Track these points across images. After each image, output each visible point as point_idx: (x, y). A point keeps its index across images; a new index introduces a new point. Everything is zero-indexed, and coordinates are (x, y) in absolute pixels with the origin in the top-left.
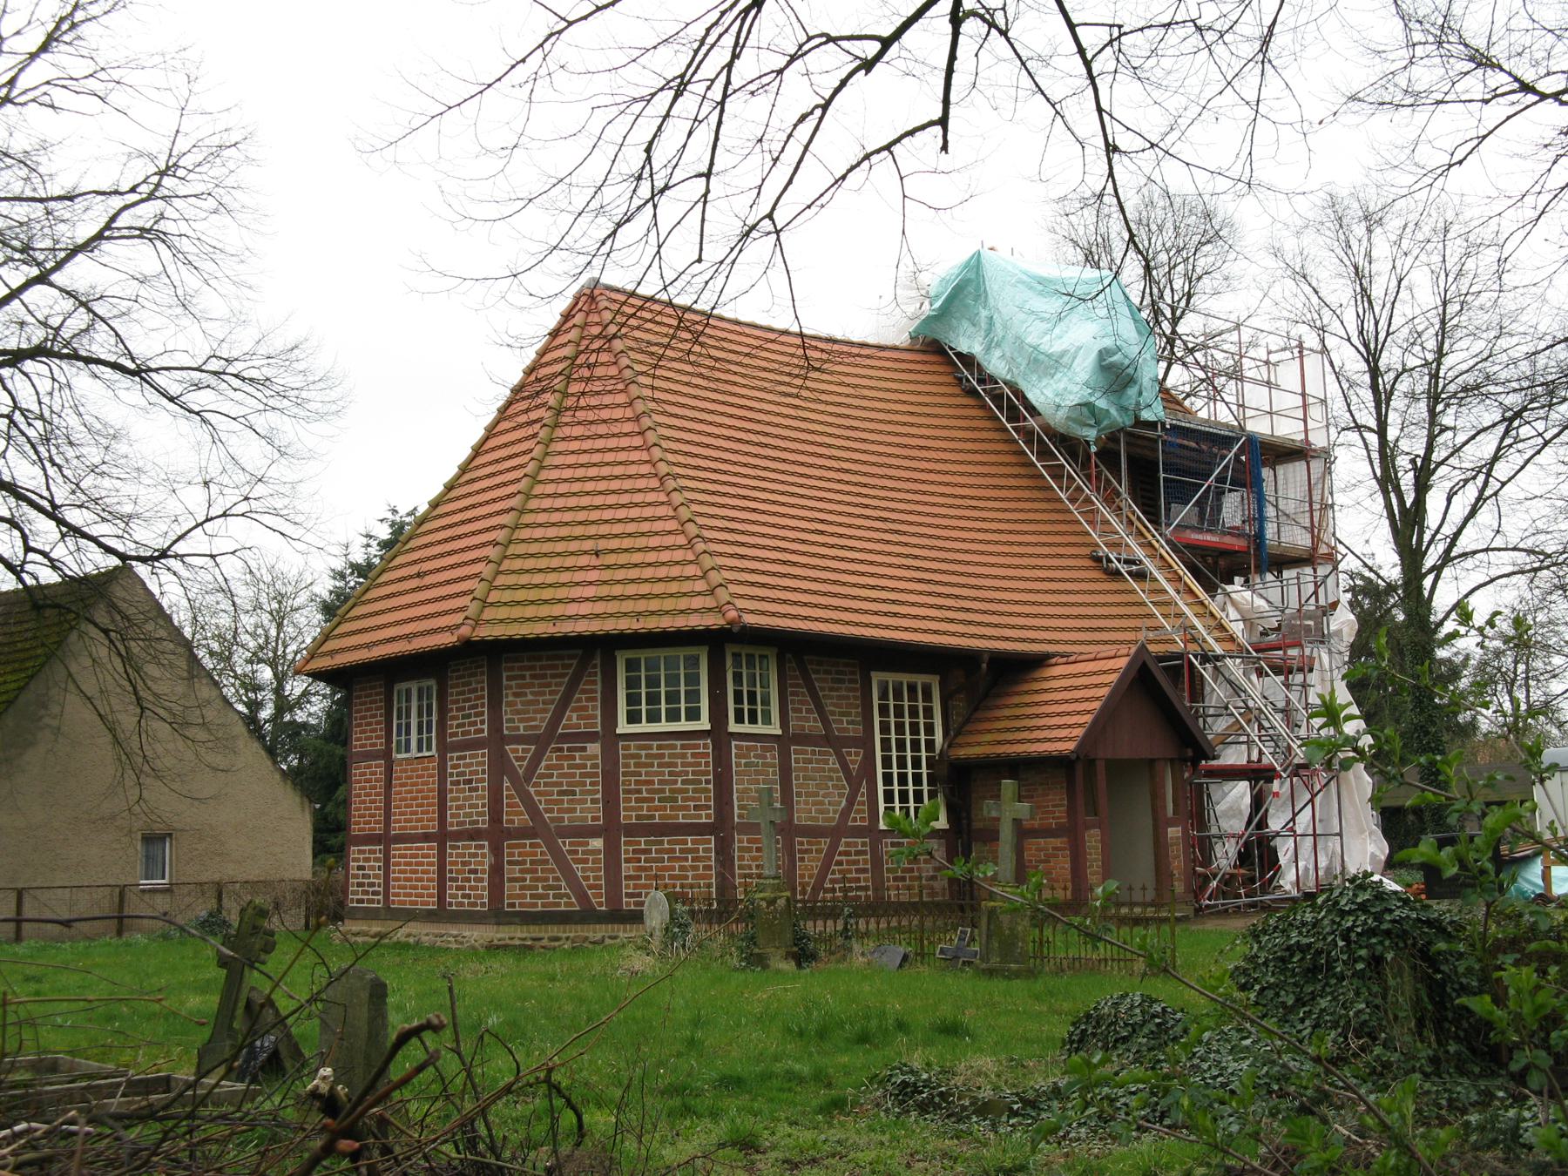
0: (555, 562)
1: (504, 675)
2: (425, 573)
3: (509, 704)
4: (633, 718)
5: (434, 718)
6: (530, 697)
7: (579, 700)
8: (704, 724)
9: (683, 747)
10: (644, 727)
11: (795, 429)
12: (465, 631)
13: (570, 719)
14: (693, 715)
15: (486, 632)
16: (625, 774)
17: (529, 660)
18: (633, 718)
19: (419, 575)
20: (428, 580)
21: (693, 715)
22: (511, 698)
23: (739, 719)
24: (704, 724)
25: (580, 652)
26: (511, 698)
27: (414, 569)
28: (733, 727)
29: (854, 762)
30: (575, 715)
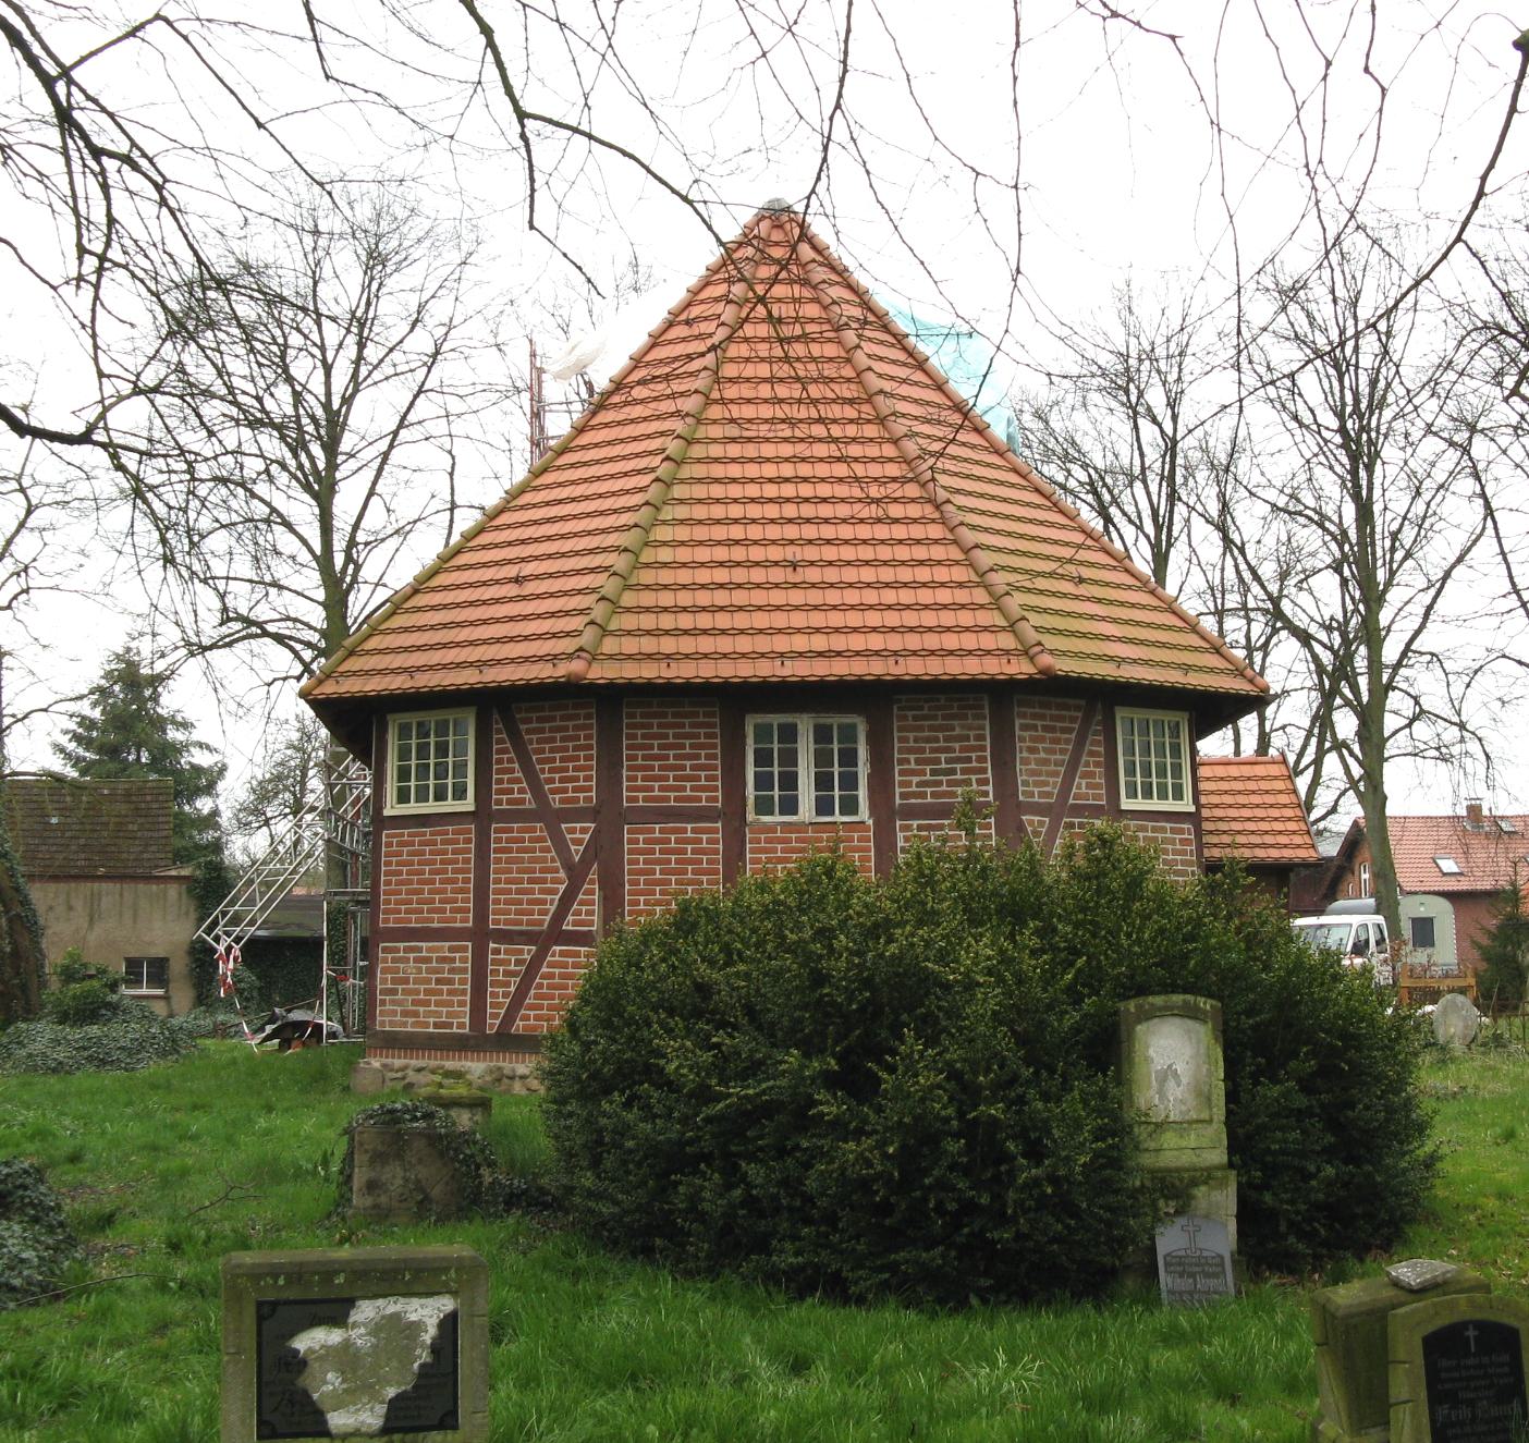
0: (704, 621)
1: (1018, 723)
2: (526, 579)
3: (1025, 762)
4: (403, 797)
5: (863, 771)
6: (1042, 755)
7: (1087, 764)
8: (468, 805)
9: (694, 831)
10: (413, 808)
11: (471, 604)
12: (576, 666)
13: (1079, 787)
14: (460, 793)
15: (600, 673)
16: (631, 852)
17: (675, 715)
18: (403, 797)
19: (517, 580)
20: (530, 588)
21: (1178, 795)
22: (1025, 754)
23: (1132, 794)
24: (468, 805)
25: (1083, 703)
26: (1025, 754)
27: (512, 571)
28: (1127, 804)
29: (578, 842)
30: (1084, 782)
